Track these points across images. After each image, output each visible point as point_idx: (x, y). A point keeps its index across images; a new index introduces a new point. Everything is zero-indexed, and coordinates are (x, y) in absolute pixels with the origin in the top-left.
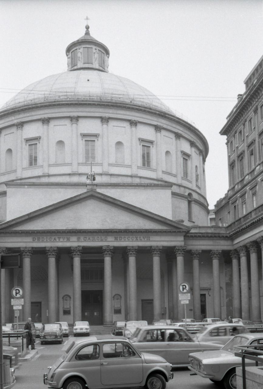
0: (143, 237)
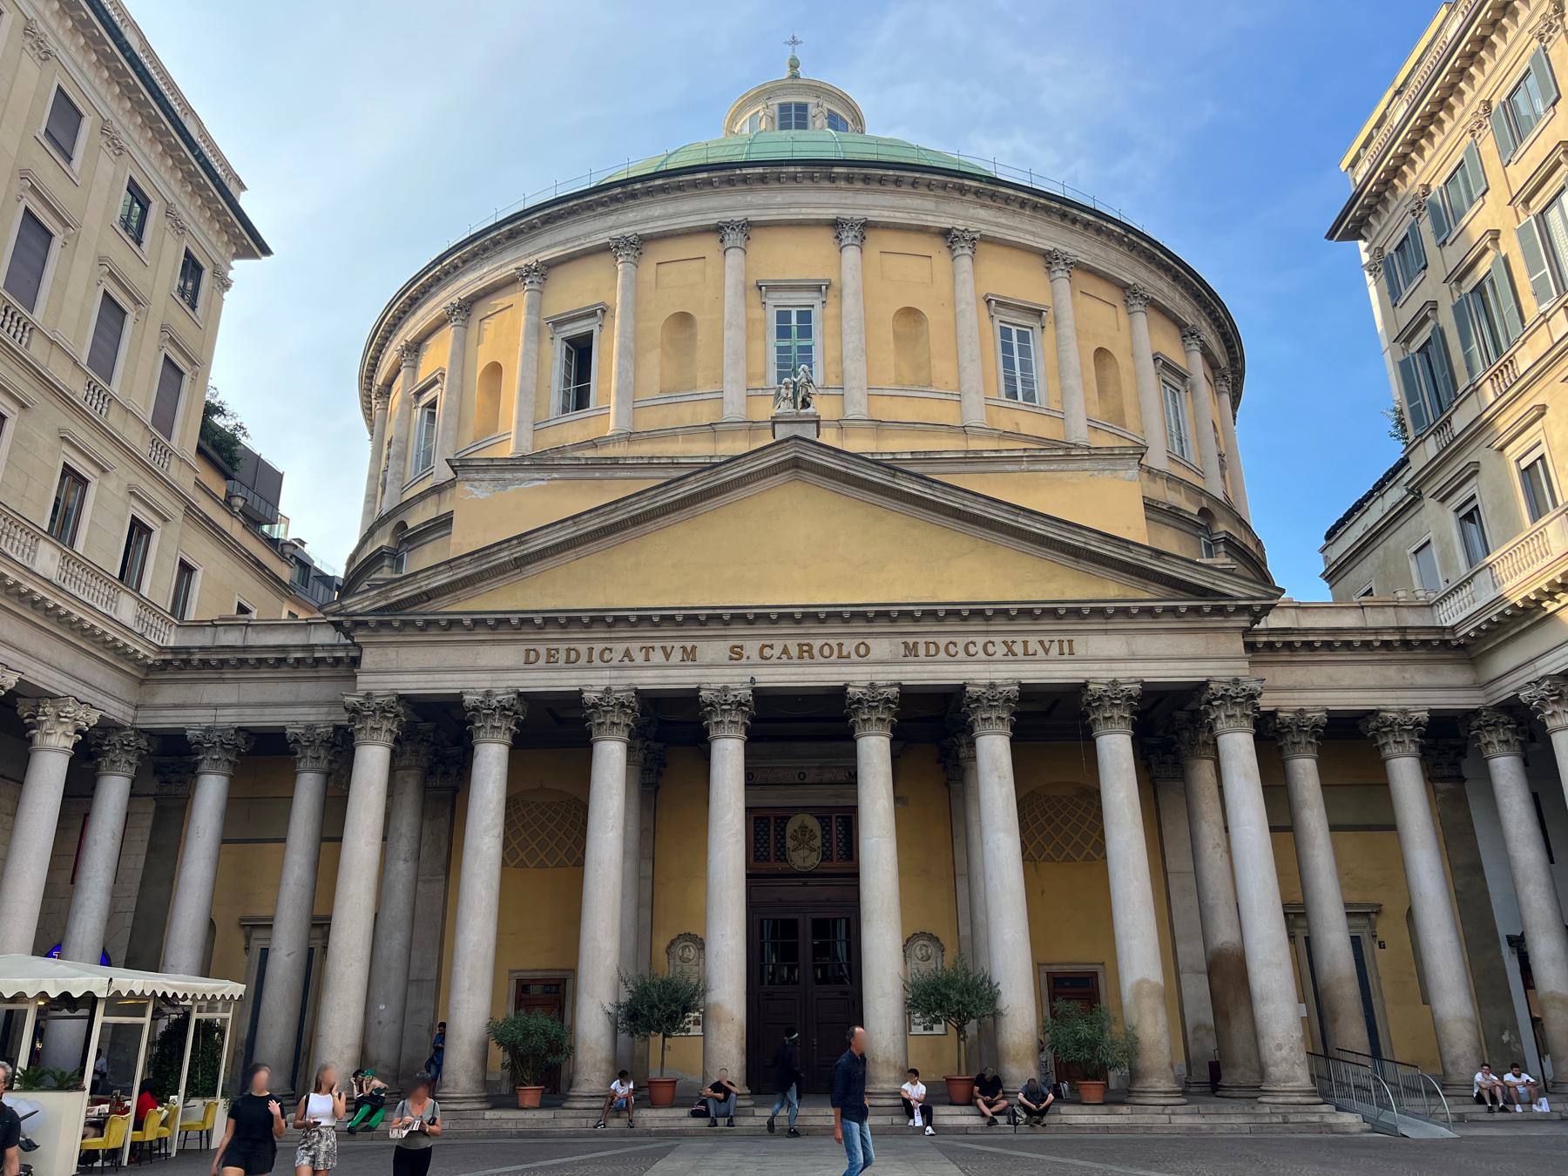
0: (1041, 642)
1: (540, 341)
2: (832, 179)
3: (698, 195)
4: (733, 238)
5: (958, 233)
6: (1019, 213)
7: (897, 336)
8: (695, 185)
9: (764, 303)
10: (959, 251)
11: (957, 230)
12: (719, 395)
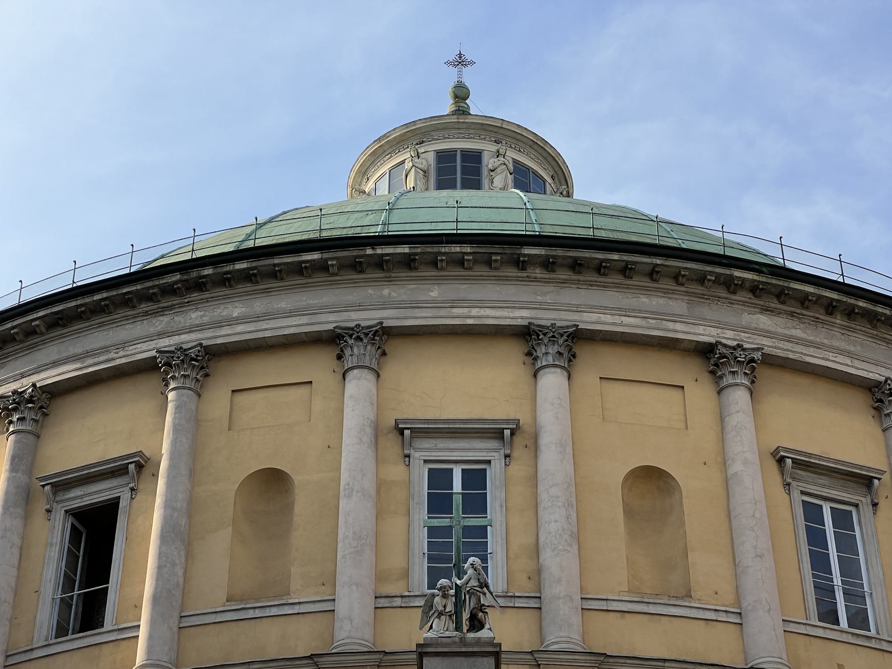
1: (27, 517)
2: (521, 264)
3: (304, 286)
4: (356, 352)
5: (724, 350)
6: (823, 323)
7: (629, 513)
8: (300, 270)
9: (408, 456)
10: (729, 380)
11: (725, 346)
12: (327, 606)
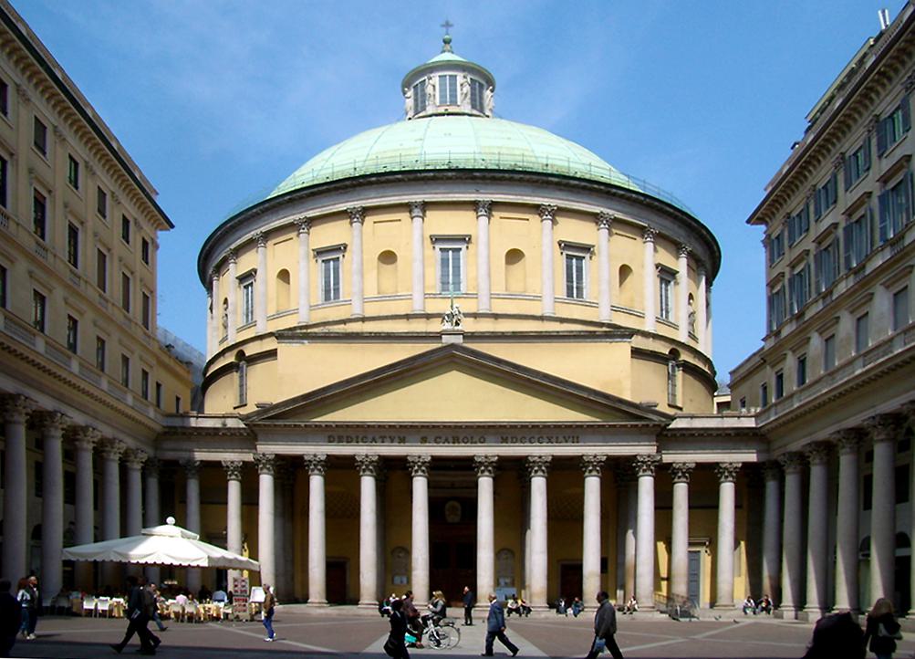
2: (474, 178)
